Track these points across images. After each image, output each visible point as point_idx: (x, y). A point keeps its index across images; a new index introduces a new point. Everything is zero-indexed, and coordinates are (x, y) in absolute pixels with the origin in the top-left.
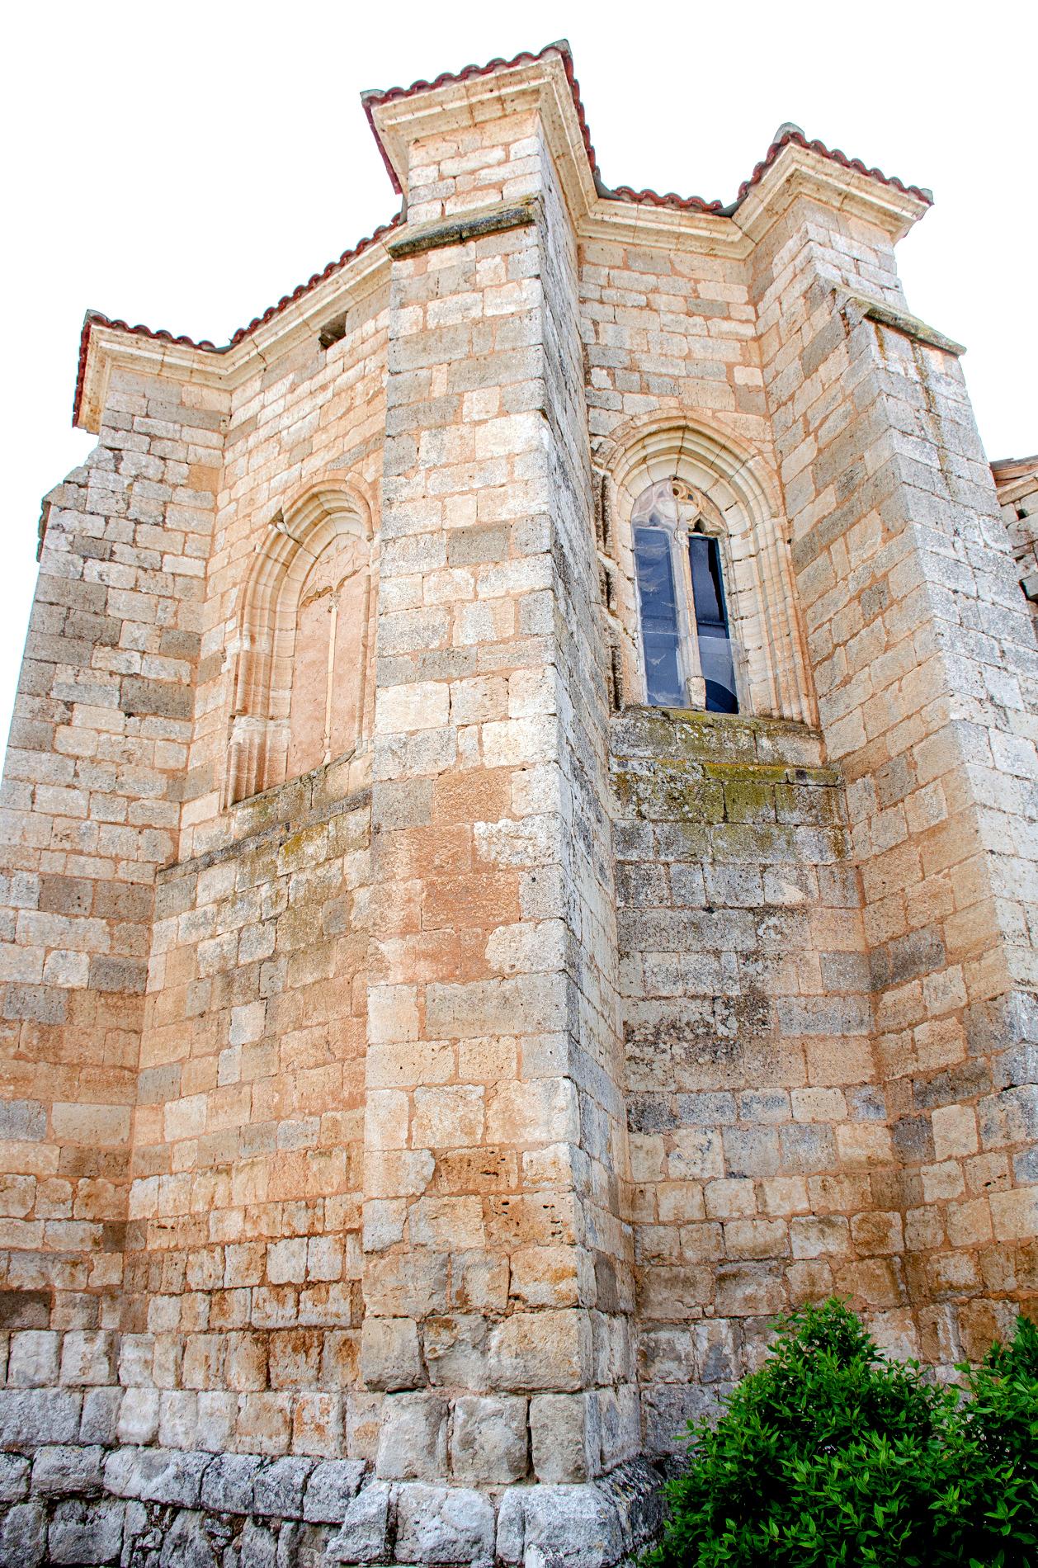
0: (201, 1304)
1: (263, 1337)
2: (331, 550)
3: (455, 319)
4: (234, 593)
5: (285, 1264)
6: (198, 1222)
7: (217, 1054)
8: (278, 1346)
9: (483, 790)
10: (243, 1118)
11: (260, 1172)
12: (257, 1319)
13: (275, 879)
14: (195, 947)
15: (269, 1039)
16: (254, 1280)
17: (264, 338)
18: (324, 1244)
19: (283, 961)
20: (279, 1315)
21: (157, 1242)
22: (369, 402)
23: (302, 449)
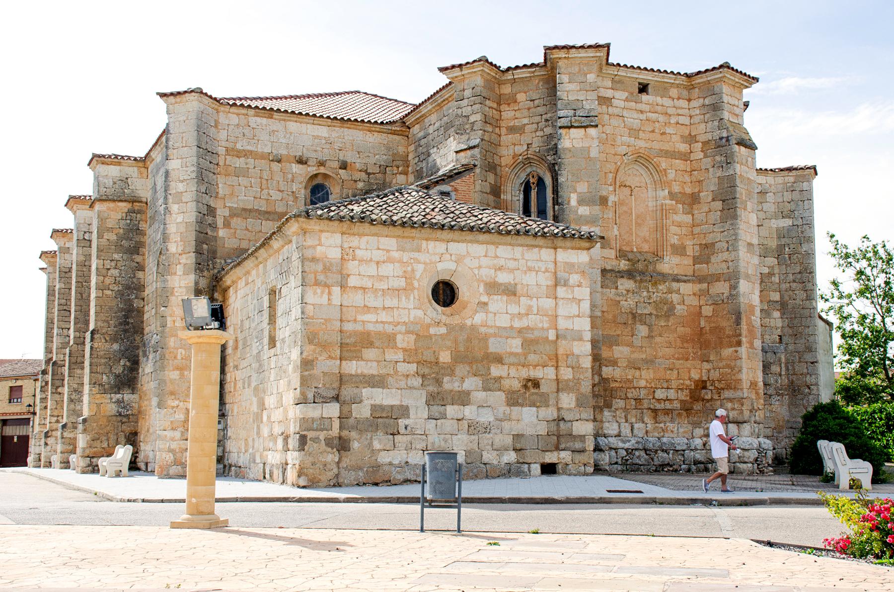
0: (633, 402)
1: (655, 411)
2: (630, 172)
3: (745, 175)
4: (611, 176)
5: (660, 394)
6: (628, 380)
7: (632, 336)
8: (660, 413)
9: (752, 307)
10: (644, 356)
11: (651, 371)
12: (652, 407)
13: (648, 292)
14: (619, 302)
15: (650, 337)
16: (651, 397)
17: (622, 72)
18: (672, 391)
19: (653, 317)
20: (658, 406)
21: (613, 385)
22: (662, 134)
23: (634, 132)
